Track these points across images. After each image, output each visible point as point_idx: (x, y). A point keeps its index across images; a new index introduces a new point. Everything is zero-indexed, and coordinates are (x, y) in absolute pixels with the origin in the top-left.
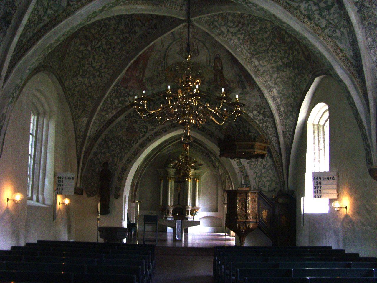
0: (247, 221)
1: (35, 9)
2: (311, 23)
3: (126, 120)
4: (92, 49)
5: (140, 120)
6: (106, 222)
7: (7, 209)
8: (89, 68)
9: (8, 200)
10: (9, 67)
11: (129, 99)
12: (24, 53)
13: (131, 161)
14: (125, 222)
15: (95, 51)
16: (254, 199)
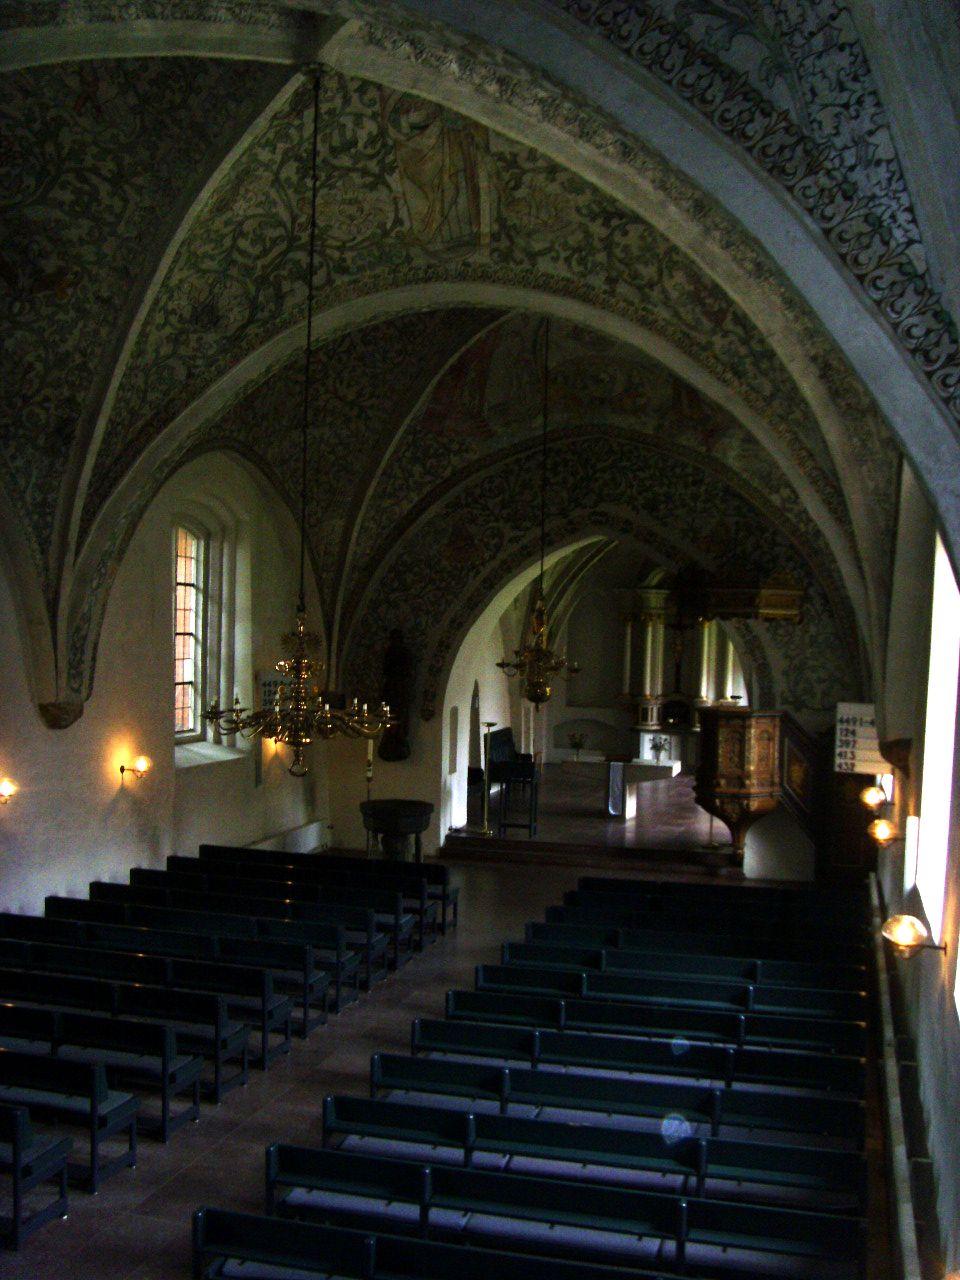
0: (743, 791)
1: (118, 400)
2: (741, 385)
3: (447, 514)
4: (331, 358)
5: (483, 513)
6: (394, 784)
7: (123, 790)
8: (331, 401)
9: (122, 769)
10: (82, 520)
11: (449, 462)
12: (111, 487)
13: (461, 625)
14: (455, 776)
15: (340, 359)
16: (767, 731)
